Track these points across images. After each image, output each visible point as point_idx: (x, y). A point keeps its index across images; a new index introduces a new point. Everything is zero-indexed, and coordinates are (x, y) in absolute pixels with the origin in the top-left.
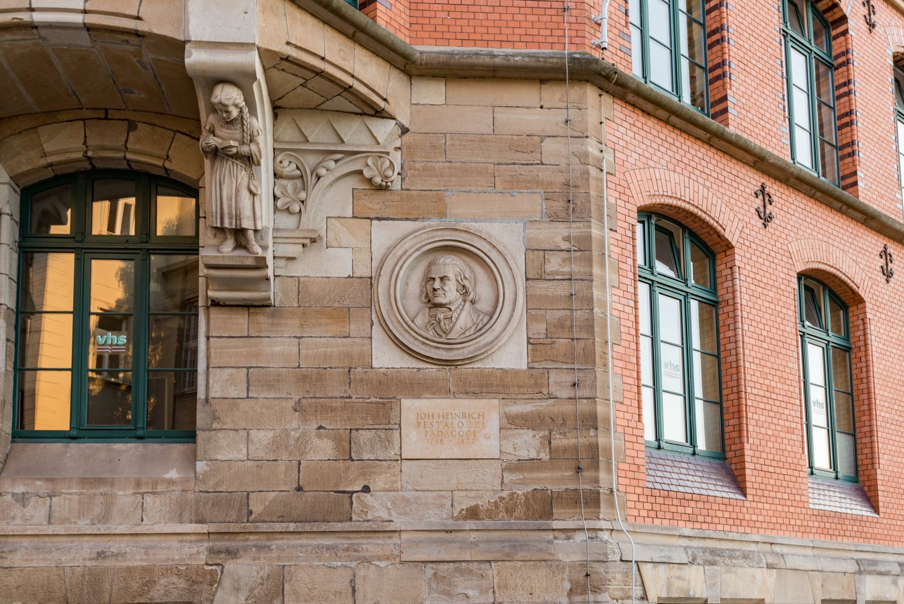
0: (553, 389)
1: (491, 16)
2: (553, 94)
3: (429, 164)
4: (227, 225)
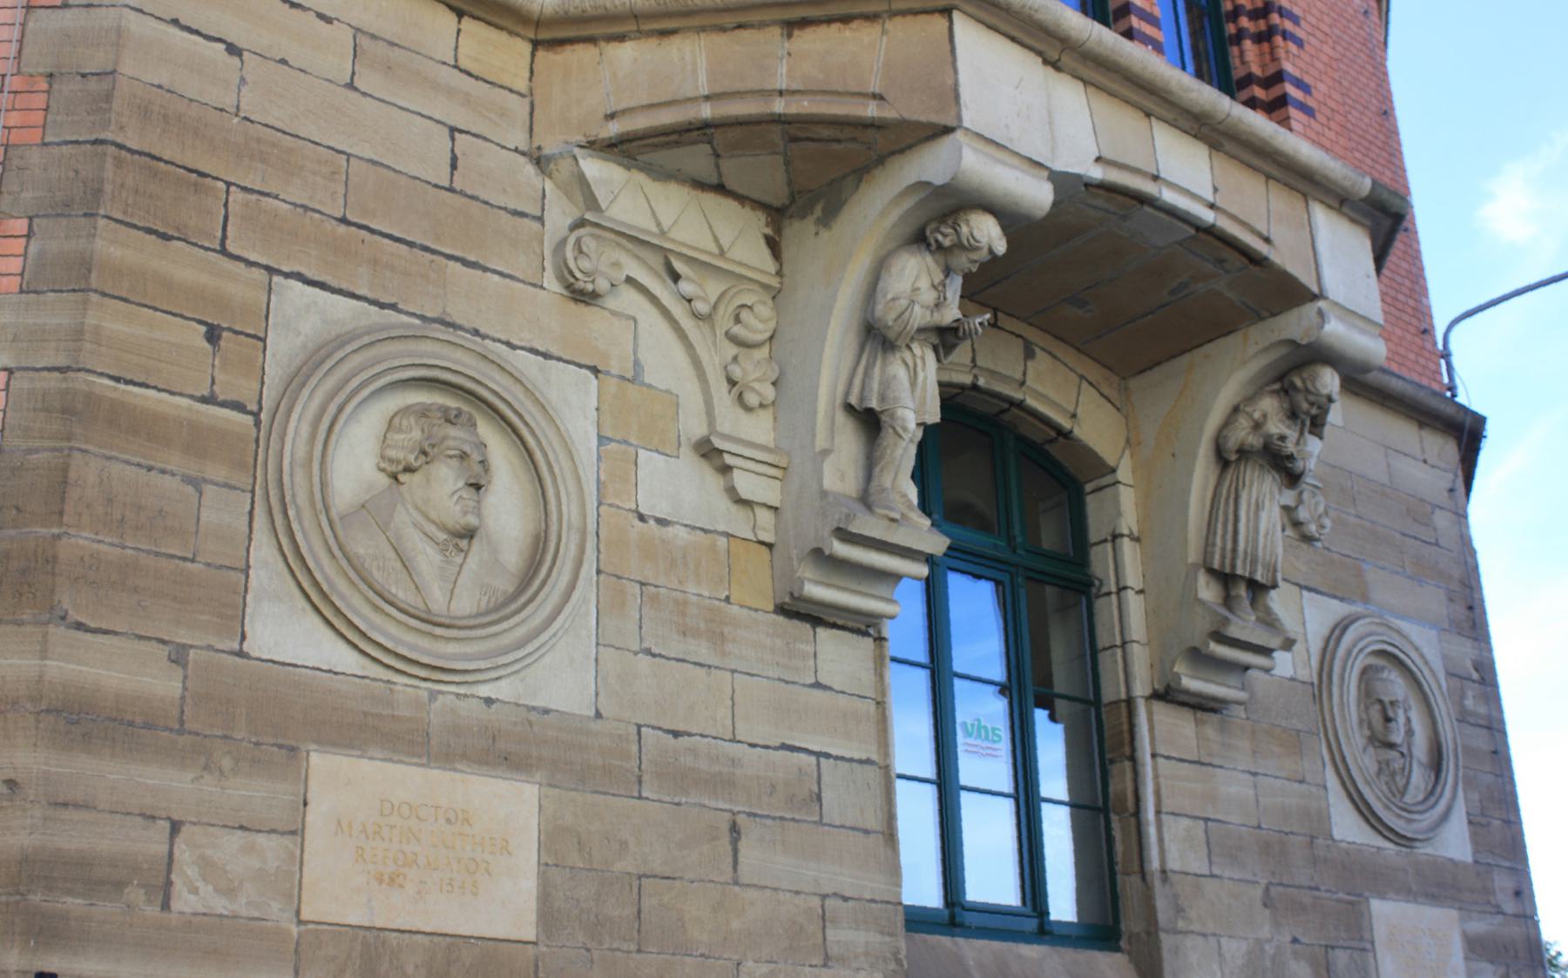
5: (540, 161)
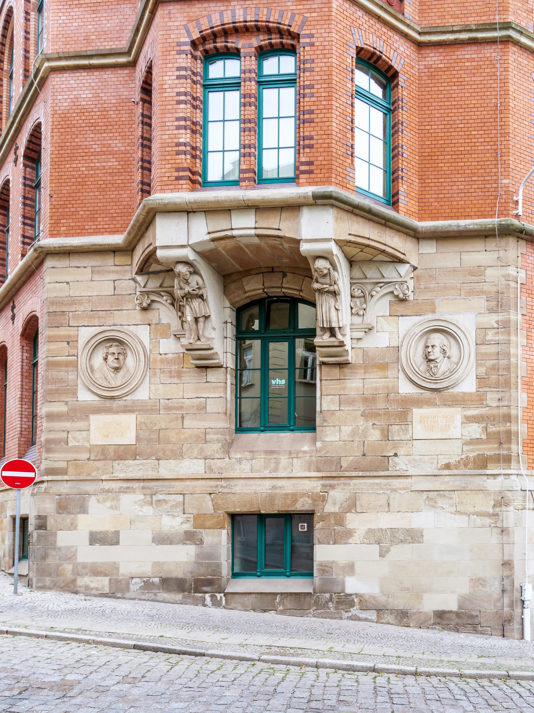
0: (489, 402)
1: (460, 203)
2: (491, 244)
4: (325, 326)
5: (134, 280)
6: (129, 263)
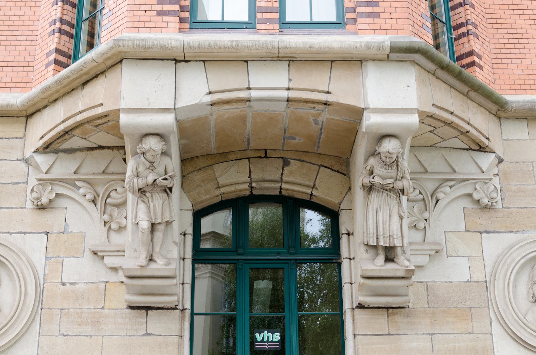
3: (522, 187)
5: (26, 161)
6: (21, 135)
